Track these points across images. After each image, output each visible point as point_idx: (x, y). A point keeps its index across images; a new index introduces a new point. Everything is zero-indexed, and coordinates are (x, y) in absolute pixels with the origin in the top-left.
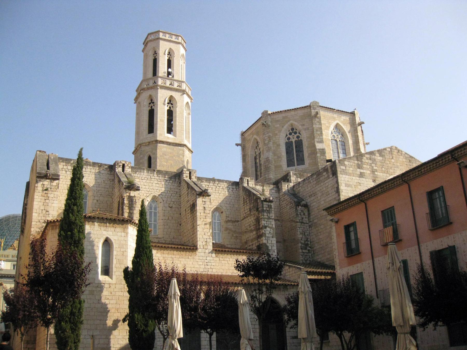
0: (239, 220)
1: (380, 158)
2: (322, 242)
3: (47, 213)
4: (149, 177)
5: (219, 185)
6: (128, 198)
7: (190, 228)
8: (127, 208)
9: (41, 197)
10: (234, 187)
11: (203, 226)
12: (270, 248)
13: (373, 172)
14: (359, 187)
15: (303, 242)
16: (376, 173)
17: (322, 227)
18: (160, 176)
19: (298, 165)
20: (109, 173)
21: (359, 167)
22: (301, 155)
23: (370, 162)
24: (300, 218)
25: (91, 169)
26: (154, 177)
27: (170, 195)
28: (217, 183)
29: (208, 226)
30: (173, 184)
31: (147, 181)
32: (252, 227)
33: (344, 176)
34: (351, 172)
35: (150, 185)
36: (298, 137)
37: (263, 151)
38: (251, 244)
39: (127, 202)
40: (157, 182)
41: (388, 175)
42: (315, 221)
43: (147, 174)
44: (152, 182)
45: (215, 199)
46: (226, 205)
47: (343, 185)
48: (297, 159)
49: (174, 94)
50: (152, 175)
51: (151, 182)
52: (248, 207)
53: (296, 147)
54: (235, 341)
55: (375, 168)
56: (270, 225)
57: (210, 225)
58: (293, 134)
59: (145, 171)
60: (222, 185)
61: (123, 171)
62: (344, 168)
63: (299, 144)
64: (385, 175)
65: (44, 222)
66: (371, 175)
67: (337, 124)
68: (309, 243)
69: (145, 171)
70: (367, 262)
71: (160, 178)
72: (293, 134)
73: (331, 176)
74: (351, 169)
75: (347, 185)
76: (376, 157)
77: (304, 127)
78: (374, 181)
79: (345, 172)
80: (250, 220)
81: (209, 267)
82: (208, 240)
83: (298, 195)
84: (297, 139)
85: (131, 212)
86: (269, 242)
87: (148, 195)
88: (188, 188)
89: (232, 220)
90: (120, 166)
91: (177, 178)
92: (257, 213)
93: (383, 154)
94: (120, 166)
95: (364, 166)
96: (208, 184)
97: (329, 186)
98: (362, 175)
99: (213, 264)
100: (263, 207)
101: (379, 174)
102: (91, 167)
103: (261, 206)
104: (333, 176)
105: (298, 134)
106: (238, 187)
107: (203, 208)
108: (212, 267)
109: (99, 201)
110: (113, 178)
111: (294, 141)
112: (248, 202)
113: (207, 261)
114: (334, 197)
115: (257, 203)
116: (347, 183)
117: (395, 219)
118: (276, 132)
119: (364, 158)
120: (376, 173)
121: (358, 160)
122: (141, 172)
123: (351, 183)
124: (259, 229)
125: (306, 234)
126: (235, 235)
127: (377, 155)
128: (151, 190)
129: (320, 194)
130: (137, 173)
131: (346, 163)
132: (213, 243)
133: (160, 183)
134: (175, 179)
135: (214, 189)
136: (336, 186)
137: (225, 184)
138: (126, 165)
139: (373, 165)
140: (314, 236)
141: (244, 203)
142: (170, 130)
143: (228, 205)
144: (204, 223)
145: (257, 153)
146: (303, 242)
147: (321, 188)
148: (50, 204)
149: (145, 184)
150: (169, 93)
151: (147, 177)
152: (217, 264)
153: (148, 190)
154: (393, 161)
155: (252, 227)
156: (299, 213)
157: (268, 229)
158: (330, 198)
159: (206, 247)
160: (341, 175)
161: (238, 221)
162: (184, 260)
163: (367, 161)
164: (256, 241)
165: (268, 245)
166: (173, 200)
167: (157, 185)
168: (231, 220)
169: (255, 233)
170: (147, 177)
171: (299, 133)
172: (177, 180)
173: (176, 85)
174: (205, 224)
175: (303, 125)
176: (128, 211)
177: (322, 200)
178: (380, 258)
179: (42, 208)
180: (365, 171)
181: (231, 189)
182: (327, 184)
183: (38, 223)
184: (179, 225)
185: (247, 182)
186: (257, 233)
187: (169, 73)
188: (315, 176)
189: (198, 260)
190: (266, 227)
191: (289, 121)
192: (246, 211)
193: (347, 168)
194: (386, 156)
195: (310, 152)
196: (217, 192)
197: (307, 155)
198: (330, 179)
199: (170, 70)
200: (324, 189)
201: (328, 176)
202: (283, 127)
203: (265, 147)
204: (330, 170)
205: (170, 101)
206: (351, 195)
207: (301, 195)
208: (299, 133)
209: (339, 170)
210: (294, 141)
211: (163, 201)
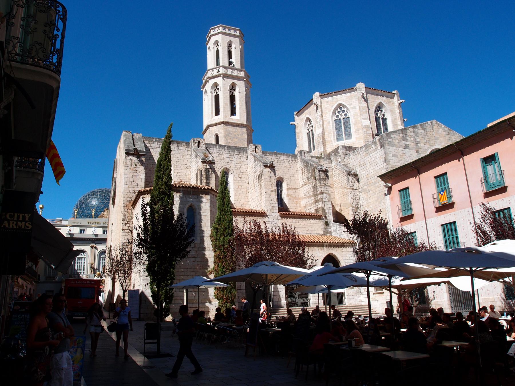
0: (298, 187)
1: (423, 131)
2: (371, 206)
3: (136, 184)
5: (281, 158)
7: (257, 195)
8: (205, 178)
9: (130, 171)
12: (327, 211)
13: (416, 143)
14: (404, 157)
15: (354, 206)
16: (419, 145)
17: (371, 192)
19: (346, 139)
20: (187, 149)
21: (404, 139)
22: (349, 132)
23: (413, 134)
24: (351, 185)
28: (279, 156)
29: (274, 193)
32: (310, 194)
33: (391, 147)
34: (397, 144)
35: (222, 158)
36: (346, 115)
37: (315, 127)
38: (309, 208)
40: (226, 156)
41: (429, 146)
42: (365, 187)
46: (287, 175)
47: (391, 155)
48: (345, 135)
49: (236, 81)
52: (306, 176)
53: (344, 124)
55: (418, 140)
56: (326, 192)
58: (341, 112)
61: (199, 147)
62: (390, 140)
63: (347, 121)
64: (427, 146)
65: (134, 192)
66: (415, 147)
67: (380, 103)
68: (359, 206)
70: (420, 222)
72: (341, 112)
73: (379, 148)
74: (397, 141)
75: (394, 156)
76: (418, 131)
77: (351, 106)
78: (417, 152)
79: (391, 144)
80: (308, 187)
82: (274, 205)
83: (348, 165)
84: (344, 117)
85: (208, 182)
86: (326, 206)
88: (255, 160)
92: (314, 181)
93: (425, 127)
95: (408, 138)
96: (271, 157)
97: (378, 157)
98: (406, 147)
100: (320, 176)
101: (421, 145)
103: (318, 175)
104: (381, 147)
105: (345, 113)
109: (179, 174)
110: (190, 153)
111: (342, 118)
114: (382, 166)
115: (315, 172)
116: (395, 154)
117: (448, 183)
119: (408, 131)
120: (419, 145)
121: (403, 134)
123: (397, 154)
124: (317, 195)
125: (357, 199)
126: (295, 201)
127: (420, 128)
129: (369, 164)
131: (393, 136)
132: (278, 208)
136: (384, 156)
137: (285, 156)
139: (416, 137)
140: (364, 201)
142: (233, 112)
144: (270, 190)
145: (310, 130)
146: (354, 206)
147: (370, 158)
148: (138, 177)
150: (231, 81)
154: (434, 133)
155: (310, 194)
156: (350, 181)
157: (325, 194)
158: (379, 168)
159: (272, 211)
160: (388, 147)
163: (411, 134)
164: (314, 205)
165: (325, 208)
167: (228, 159)
169: (313, 198)
171: (347, 112)
172: (245, 154)
173: (236, 73)
174: (272, 191)
175: (351, 104)
176: (205, 181)
177: (371, 169)
178: (433, 219)
179: (132, 180)
180: (409, 143)
182: (375, 155)
183: (129, 193)
186: (315, 199)
187: (230, 63)
188: (364, 149)
190: (322, 193)
191: (337, 101)
192: (305, 180)
193: (394, 141)
194: (427, 130)
195: (357, 128)
196: (278, 163)
197: (354, 130)
198: (379, 151)
200: (373, 159)
201: (377, 148)
202: (332, 106)
203: (317, 125)
204: (378, 143)
205: (233, 87)
206: (398, 165)
207: (351, 165)
208: (347, 112)
209: (387, 142)
210: (342, 118)
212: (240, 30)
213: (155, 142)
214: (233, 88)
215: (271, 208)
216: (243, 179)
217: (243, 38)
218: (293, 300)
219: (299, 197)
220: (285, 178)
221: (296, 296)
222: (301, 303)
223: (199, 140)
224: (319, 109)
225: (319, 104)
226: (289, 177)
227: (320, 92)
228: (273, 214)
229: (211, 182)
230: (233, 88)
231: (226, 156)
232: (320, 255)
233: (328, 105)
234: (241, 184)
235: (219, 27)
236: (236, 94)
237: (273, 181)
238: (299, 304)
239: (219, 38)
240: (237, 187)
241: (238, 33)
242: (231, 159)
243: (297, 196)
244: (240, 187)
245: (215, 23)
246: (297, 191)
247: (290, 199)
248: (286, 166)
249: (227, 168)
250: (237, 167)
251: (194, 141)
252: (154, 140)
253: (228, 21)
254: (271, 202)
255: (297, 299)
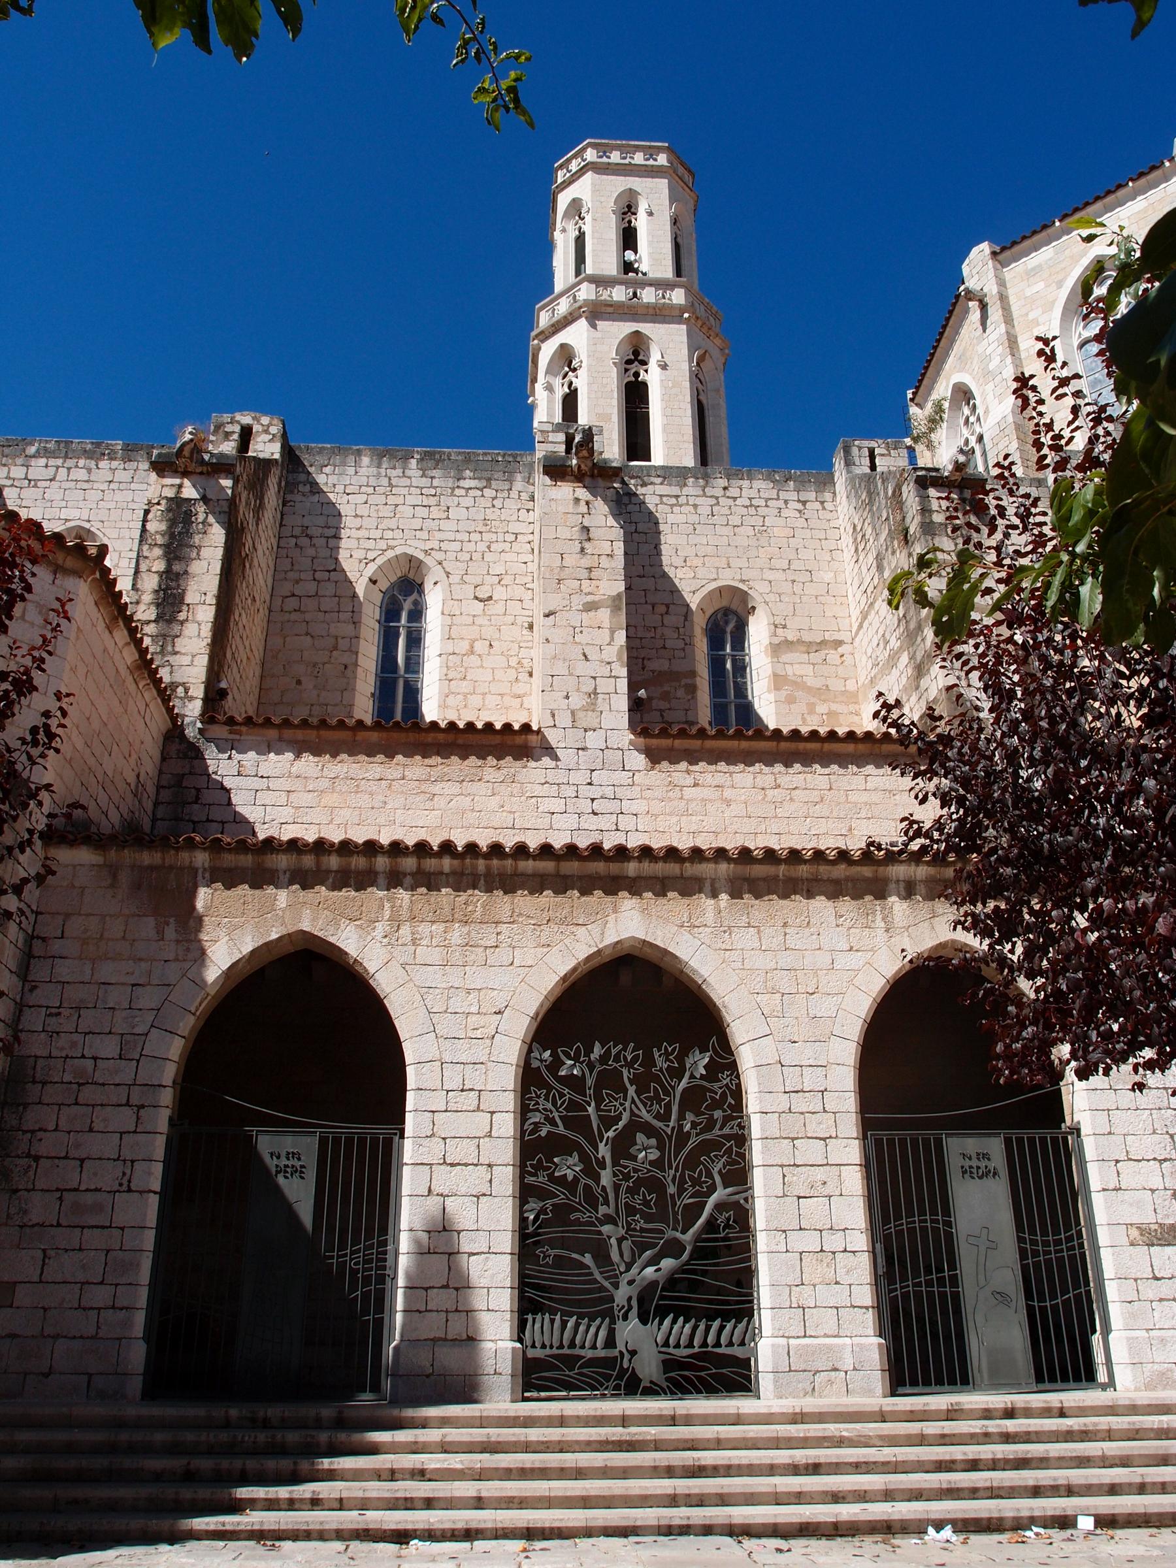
4: (385, 482)
5: (733, 492)
6: (169, 510)
8: (158, 552)
10: (812, 495)
11: (576, 618)
18: (435, 473)
25: (113, 470)
26: (407, 482)
27: (482, 547)
28: (723, 482)
30: (498, 503)
31: (373, 499)
32: (893, 640)
35: (386, 511)
39: (163, 527)
43: (374, 470)
44: (400, 500)
45: (710, 550)
46: (769, 575)
49: (645, 328)
50: (399, 472)
51: (391, 500)
54: (667, 1263)
57: (615, 609)
59: (366, 460)
60: (745, 493)
69: (366, 460)
71: (436, 482)
81: (606, 822)
82: (604, 686)
87: (371, 555)
89: (807, 637)
90: (227, 435)
91: (519, 477)
94: (227, 435)
96: (675, 490)
99: (634, 807)
102: (115, 464)
106: (828, 496)
107: (576, 533)
108: (626, 822)
112: (869, 531)
113: (594, 792)
118: (1031, 316)
122: (344, 464)
128: (389, 534)
130: (327, 470)
133: (432, 501)
134: (511, 481)
135: (705, 510)
138: (256, 428)
141: (856, 550)
143: (780, 575)
144: (578, 601)
149: (363, 510)
151: (372, 481)
152: (656, 807)
153: (378, 534)
155: (893, 640)
159: (589, 719)
161: (839, 643)
162: (454, 788)
166: (498, 569)
167: (423, 512)
168: (800, 642)
170: (372, 481)
172: (519, 484)
173: (648, 296)
174: (590, 607)
176: (160, 566)
181: (794, 505)
184: (524, 676)
185: (867, 462)
186: (912, 657)
187: (628, 267)
189: (539, 790)
199: (629, 255)
202: (1060, 285)
205: (636, 353)
211: (448, 574)
212: (670, 150)
213: (36, 456)
214: (635, 354)
215: (577, 701)
216: (498, 608)
217: (687, 174)
218: (590, 1338)
219: (851, 686)
220: (758, 592)
221: (622, 1294)
222: (669, 1364)
223: (246, 419)
224: (995, 313)
225: (991, 289)
226: (786, 587)
227: (992, 241)
228: (594, 740)
229: (196, 567)
230: (635, 354)
231: (411, 500)
232: (855, 960)
233: (1041, 285)
234: (489, 632)
235: (584, 149)
236: (653, 377)
237: (606, 548)
238: (648, 1367)
239: (584, 189)
240: (464, 646)
241: (662, 159)
242: (436, 513)
243: (836, 685)
244: (480, 647)
245: (567, 143)
246: (833, 656)
247: (790, 700)
248: (763, 530)
249: (411, 559)
250: (471, 547)
251: (218, 427)
252: (32, 450)
253: (618, 124)
254: (582, 668)
255: (630, 1331)
